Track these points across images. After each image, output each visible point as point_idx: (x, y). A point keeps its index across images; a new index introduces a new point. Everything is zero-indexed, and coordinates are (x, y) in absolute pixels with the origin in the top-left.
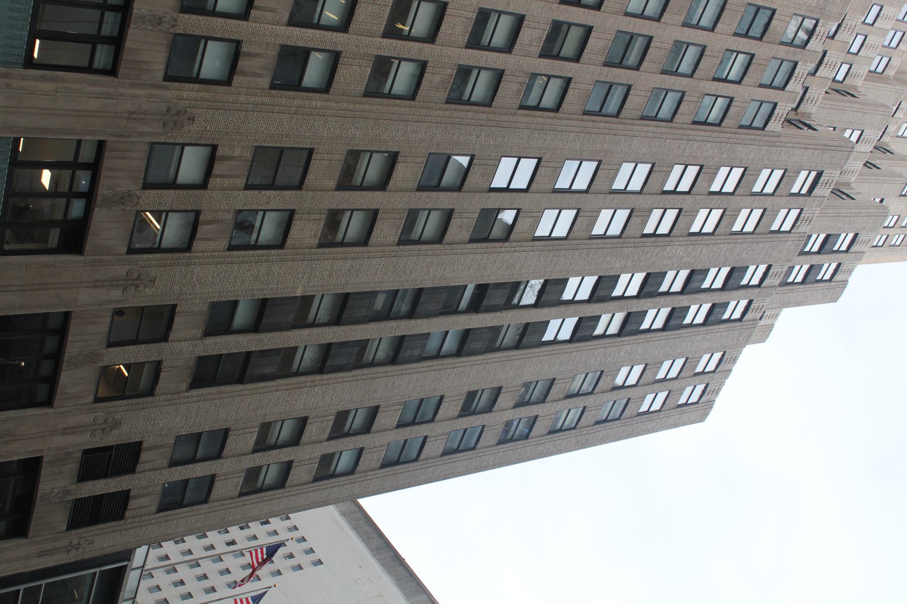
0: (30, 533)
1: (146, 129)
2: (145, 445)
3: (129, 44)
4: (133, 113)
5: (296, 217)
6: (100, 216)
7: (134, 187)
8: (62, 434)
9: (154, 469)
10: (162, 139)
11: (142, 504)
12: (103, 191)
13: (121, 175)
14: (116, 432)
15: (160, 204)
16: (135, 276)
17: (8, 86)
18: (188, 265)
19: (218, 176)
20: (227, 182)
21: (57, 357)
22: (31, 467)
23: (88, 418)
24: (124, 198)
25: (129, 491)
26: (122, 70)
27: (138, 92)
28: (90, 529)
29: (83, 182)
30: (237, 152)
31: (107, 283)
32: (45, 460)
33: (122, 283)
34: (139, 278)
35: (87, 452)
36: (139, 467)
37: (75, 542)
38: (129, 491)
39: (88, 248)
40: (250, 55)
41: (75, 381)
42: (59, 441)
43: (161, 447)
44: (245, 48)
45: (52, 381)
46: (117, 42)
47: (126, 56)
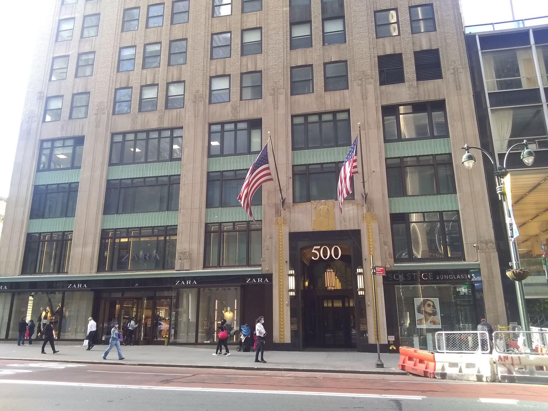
0: (441, 98)
1: (202, 109)
2: (381, 54)
3: (170, 126)
4: (195, 116)
5: (245, 28)
6: (243, 116)
7: (229, 105)
8: (366, 99)
9: (400, 43)
10: (207, 101)
11: (424, 42)
12: (230, 118)
13: (224, 112)
14: (369, 72)
15: (237, 92)
16: (272, 91)
17: (185, 164)
18: (268, 69)
19: (224, 71)
20: (228, 66)
21: (320, 114)
22: (390, 110)
23: (357, 89)
24: (233, 109)
25: (416, 53)
26: (181, 125)
27: (187, 116)
28: (442, 66)
29: (231, 127)
30: (213, 67)
31: (276, 103)
32: (385, 103)
33: (276, 96)
34: (274, 89)
35: (382, 83)
36: (397, 52)
37: (452, 71)
38: (416, 53)
39: (259, 117)
40: (172, 78)
41: (333, 100)
42: (371, 100)
43: (384, 45)
44: (170, 81)
45: (334, 113)
46: (172, 129)
47: (174, 125)
